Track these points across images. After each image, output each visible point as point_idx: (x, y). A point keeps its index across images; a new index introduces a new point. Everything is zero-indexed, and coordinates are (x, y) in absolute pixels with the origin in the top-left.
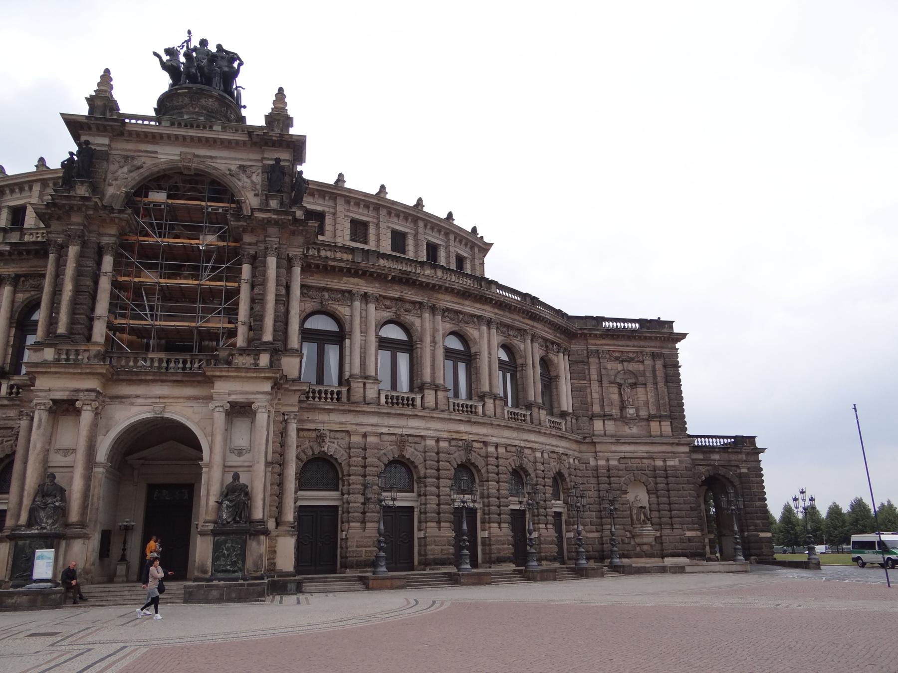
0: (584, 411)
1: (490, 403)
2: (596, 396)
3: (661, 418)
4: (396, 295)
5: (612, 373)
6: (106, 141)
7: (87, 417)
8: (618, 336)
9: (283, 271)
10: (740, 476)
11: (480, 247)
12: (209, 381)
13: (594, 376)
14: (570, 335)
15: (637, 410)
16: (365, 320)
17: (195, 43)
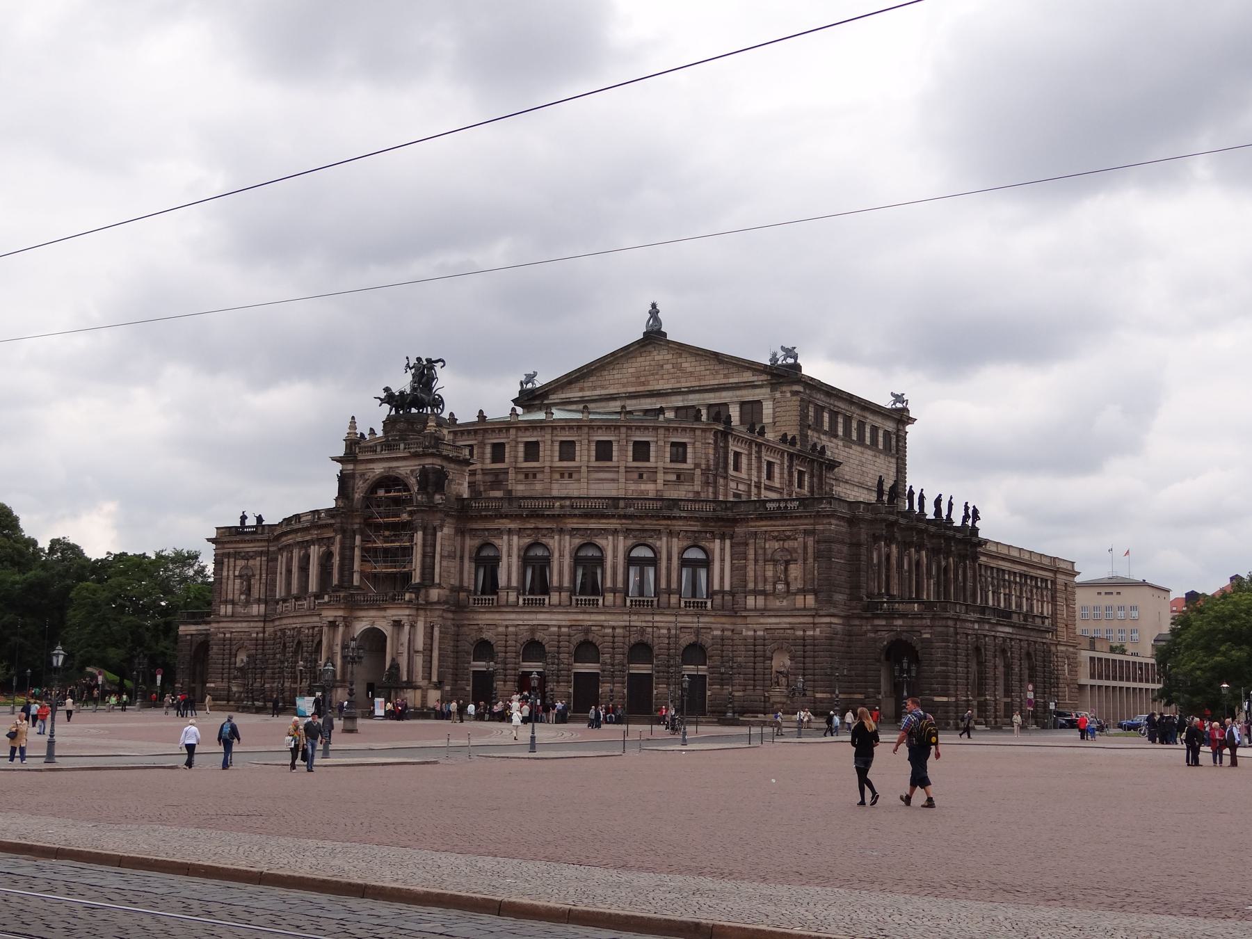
0: (740, 588)
1: (610, 597)
2: (751, 574)
3: (804, 592)
4: (532, 526)
5: (769, 552)
6: (351, 467)
7: (341, 629)
8: (771, 519)
9: (429, 537)
10: (923, 641)
11: (704, 430)
12: (385, 609)
13: (751, 557)
14: (734, 521)
15: (788, 584)
16: (510, 545)
17: (413, 362)
